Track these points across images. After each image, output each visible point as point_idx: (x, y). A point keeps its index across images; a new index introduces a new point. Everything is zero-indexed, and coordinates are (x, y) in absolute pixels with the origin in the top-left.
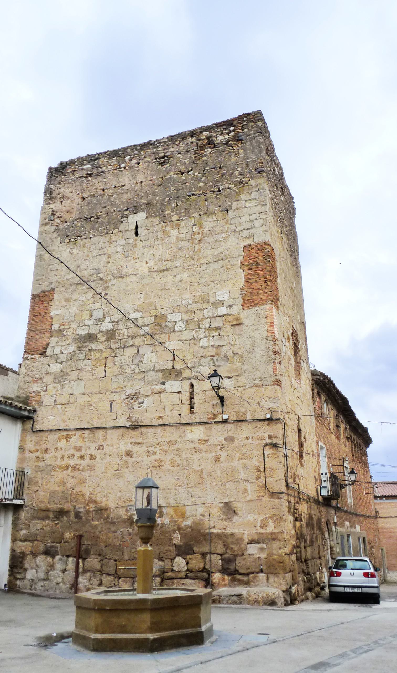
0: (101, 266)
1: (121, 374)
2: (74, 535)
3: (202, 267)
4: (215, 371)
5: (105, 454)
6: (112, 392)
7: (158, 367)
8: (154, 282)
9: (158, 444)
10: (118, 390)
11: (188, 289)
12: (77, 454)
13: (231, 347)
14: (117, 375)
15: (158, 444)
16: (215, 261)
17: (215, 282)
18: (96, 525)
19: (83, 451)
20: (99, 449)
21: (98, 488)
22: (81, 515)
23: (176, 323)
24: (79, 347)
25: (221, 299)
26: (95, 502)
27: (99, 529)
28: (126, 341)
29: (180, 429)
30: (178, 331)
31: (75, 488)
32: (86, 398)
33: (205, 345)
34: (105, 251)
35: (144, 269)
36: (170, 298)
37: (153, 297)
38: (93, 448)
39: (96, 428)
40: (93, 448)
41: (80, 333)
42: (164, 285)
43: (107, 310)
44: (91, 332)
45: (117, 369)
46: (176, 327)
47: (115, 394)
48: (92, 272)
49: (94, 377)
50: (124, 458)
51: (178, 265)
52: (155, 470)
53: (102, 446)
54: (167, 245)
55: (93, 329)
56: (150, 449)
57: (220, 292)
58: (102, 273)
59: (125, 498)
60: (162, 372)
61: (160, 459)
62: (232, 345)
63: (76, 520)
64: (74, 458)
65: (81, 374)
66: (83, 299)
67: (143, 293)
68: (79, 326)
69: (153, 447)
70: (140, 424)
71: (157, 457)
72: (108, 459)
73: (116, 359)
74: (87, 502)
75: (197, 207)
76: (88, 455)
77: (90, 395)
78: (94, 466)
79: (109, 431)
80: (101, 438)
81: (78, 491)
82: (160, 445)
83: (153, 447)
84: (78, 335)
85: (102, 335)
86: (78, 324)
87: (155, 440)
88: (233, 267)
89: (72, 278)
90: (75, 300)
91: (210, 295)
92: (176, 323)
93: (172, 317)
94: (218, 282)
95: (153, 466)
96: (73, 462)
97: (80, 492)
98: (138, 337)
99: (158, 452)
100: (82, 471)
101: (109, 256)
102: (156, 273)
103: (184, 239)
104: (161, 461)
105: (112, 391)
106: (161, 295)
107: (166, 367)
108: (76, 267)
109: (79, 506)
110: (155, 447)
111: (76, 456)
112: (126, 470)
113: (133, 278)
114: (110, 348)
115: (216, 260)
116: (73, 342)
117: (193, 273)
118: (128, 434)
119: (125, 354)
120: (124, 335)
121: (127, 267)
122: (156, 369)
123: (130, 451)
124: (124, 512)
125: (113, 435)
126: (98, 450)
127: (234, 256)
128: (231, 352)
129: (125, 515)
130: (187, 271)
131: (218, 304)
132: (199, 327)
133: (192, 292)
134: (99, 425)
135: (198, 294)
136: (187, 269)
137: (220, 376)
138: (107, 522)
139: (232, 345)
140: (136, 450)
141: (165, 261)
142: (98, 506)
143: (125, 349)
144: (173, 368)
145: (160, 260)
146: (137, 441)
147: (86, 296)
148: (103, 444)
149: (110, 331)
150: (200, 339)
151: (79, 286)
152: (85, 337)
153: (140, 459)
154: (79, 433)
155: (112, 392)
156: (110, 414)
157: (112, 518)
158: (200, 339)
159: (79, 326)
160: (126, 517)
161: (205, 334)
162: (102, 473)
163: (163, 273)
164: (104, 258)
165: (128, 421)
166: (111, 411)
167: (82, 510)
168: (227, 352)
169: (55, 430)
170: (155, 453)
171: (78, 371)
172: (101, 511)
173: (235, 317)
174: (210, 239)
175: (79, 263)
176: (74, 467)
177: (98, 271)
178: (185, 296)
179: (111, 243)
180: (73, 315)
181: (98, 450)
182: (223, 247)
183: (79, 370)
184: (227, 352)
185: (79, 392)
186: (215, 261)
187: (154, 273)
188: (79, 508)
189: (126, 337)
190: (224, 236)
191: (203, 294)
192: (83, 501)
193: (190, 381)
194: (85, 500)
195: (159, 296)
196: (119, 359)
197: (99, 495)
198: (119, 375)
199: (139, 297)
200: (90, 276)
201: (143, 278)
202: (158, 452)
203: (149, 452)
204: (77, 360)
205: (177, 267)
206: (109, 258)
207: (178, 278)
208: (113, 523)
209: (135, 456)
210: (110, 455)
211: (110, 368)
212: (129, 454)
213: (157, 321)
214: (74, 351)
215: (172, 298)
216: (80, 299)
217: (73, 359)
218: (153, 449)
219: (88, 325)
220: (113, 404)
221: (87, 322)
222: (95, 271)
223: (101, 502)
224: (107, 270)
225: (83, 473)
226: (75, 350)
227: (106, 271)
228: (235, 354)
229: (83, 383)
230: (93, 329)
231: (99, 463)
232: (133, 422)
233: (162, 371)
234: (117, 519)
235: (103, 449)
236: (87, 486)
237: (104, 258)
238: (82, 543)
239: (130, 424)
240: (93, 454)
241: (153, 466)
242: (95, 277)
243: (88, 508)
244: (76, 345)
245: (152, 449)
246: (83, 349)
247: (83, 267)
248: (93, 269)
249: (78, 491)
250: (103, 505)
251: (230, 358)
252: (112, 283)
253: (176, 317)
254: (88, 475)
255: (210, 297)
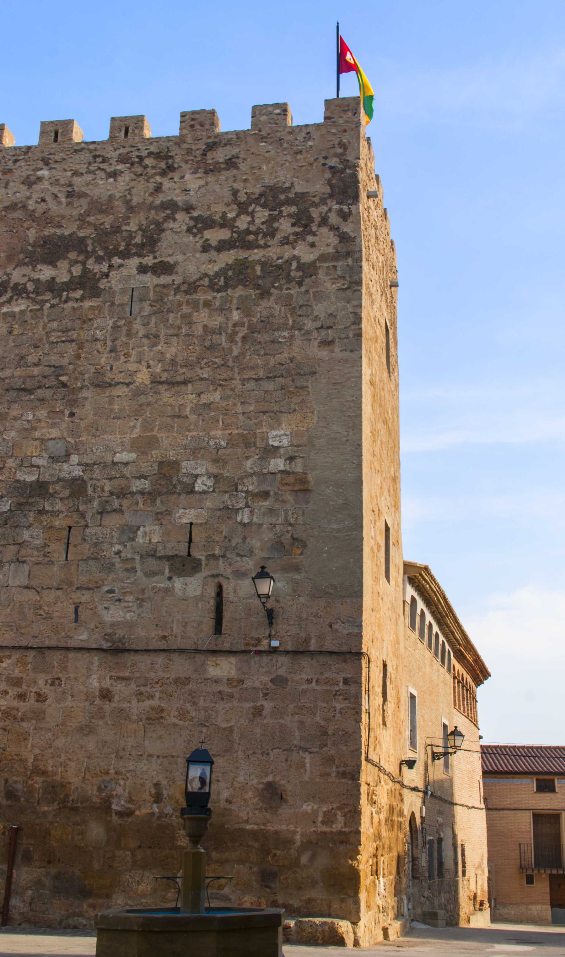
0: (65, 362)
1: (95, 558)
2: (4, 827)
3: (247, 385)
4: (263, 568)
5: (64, 693)
6: (77, 588)
7: (163, 551)
8: (160, 402)
9: (157, 683)
10: (90, 586)
11: (221, 421)
12: (13, 692)
13: (290, 528)
14: (89, 558)
15: (157, 683)
16: (268, 378)
17: (267, 415)
18: (44, 813)
19: (24, 687)
20: (52, 684)
21: (50, 751)
22: (20, 794)
23: (197, 476)
24: (20, 504)
25: (276, 444)
26: (44, 773)
27: (50, 818)
28: (107, 502)
29: (196, 659)
30: (200, 493)
31: (8, 749)
32: (31, 595)
33: (246, 520)
34: (74, 335)
35: (143, 377)
36: (187, 433)
37: (157, 428)
38: (41, 683)
39: (49, 648)
40: (41, 683)
41: (22, 479)
42: (177, 410)
43: (73, 442)
44: (42, 479)
45: (89, 550)
46: (196, 485)
47: (84, 592)
48: (48, 371)
49: (47, 559)
50: (97, 701)
51: (205, 376)
52: (150, 724)
53: (58, 679)
54: (187, 338)
55: (47, 475)
56: (143, 689)
57: (275, 433)
58: (67, 374)
59: (98, 769)
60: (168, 560)
61: (160, 706)
62: (291, 525)
63: (9, 802)
64: (8, 697)
65: (23, 552)
66: (30, 417)
67: (141, 419)
68: (21, 466)
69: (149, 686)
70: (127, 646)
71: (155, 702)
72: (69, 703)
73: (88, 531)
74: (29, 773)
75: (242, 277)
76: (32, 694)
77: (39, 589)
78: (44, 712)
79: (71, 655)
80: (56, 665)
81: (13, 753)
82: (160, 684)
83: (149, 686)
84: (18, 481)
85: (64, 487)
86: (18, 462)
87: (152, 675)
88: (301, 391)
89: (10, 378)
90: (15, 419)
91: (258, 435)
92: (197, 476)
93: (187, 466)
94: (272, 414)
95: (149, 719)
96: (5, 703)
97: (17, 755)
98: (129, 496)
99: (157, 695)
100: (22, 720)
101: (81, 347)
102: (165, 387)
103: (217, 331)
104: (162, 711)
105: (79, 586)
106: (172, 427)
107: (176, 552)
108: (17, 358)
109: (15, 778)
110: (152, 687)
111: (10, 694)
112: (101, 723)
113: (121, 391)
114: (78, 510)
115: (271, 375)
116: (8, 493)
117: (230, 393)
118: (106, 662)
119: (104, 523)
120: (103, 490)
121: (111, 368)
122: (158, 555)
123: (108, 690)
124: (95, 792)
125: (78, 661)
126: (51, 685)
127: (302, 373)
128: (289, 536)
129: (97, 796)
130: (220, 389)
131: (271, 451)
132: (237, 488)
133: (226, 426)
134: (54, 643)
135: (236, 432)
136: (220, 385)
137: (272, 578)
138: (65, 807)
139: (291, 525)
140: (119, 688)
141: (182, 366)
142: (49, 779)
143: (105, 515)
144: (189, 555)
145: (173, 362)
146: (121, 674)
147: (37, 413)
148: (60, 675)
149: (77, 480)
150: (237, 510)
151: (23, 393)
152: (31, 486)
153: (125, 705)
154: (16, 655)
155: (77, 588)
156: (74, 625)
157: (73, 801)
158: (237, 510)
159: (21, 466)
160: (98, 801)
161: (247, 503)
162: (57, 726)
163: (177, 388)
164: (71, 349)
165: (105, 639)
166: (76, 621)
167: (19, 787)
168: (282, 535)
169: (75, 648)
170: (151, 697)
171: (17, 546)
172: (55, 790)
173: (298, 477)
174: (264, 337)
175: (24, 352)
176: (8, 713)
177: (59, 370)
178: (214, 433)
179: (84, 322)
180: (10, 444)
181: (51, 685)
182: (285, 355)
183: (20, 544)
184: (282, 535)
185: (19, 584)
186: (268, 378)
187: (160, 386)
188: (15, 782)
189: (106, 494)
190: (286, 334)
191: (245, 432)
192: (22, 770)
193: (216, 580)
194: (26, 769)
195: (169, 428)
196: (93, 532)
197: (51, 762)
198: (92, 559)
199: (132, 424)
200: (45, 377)
201: (138, 393)
202: (157, 695)
203: (141, 694)
204: (16, 527)
205: (202, 379)
206: (79, 348)
207: (204, 399)
208: (74, 809)
209: (116, 698)
210: (73, 696)
211: (75, 546)
212: (106, 695)
213: (163, 471)
214: (10, 510)
215: (191, 434)
216: (24, 418)
217: (10, 523)
218: (149, 690)
219: (38, 467)
220: (80, 609)
221: (35, 461)
222: (53, 369)
223: (55, 774)
224: (75, 369)
225: (24, 724)
226: (13, 508)
227: (74, 372)
228: (295, 539)
229: (26, 568)
230: (47, 475)
231: (53, 710)
232: (114, 642)
233: (169, 558)
234: (82, 803)
235: (60, 685)
236: (29, 745)
237: (71, 349)
238: (20, 842)
239: (109, 644)
240: (41, 692)
241: (149, 719)
242: (52, 381)
243: (30, 782)
244: (14, 499)
245: (147, 689)
246: (27, 507)
247: (31, 359)
248: (49, 366)
249: (13, 753)
250: (58, 778)
251: (287, 547)
252: (83, 395)
253: (201, 467)
254: (32, 728)
255: (258, 439)
